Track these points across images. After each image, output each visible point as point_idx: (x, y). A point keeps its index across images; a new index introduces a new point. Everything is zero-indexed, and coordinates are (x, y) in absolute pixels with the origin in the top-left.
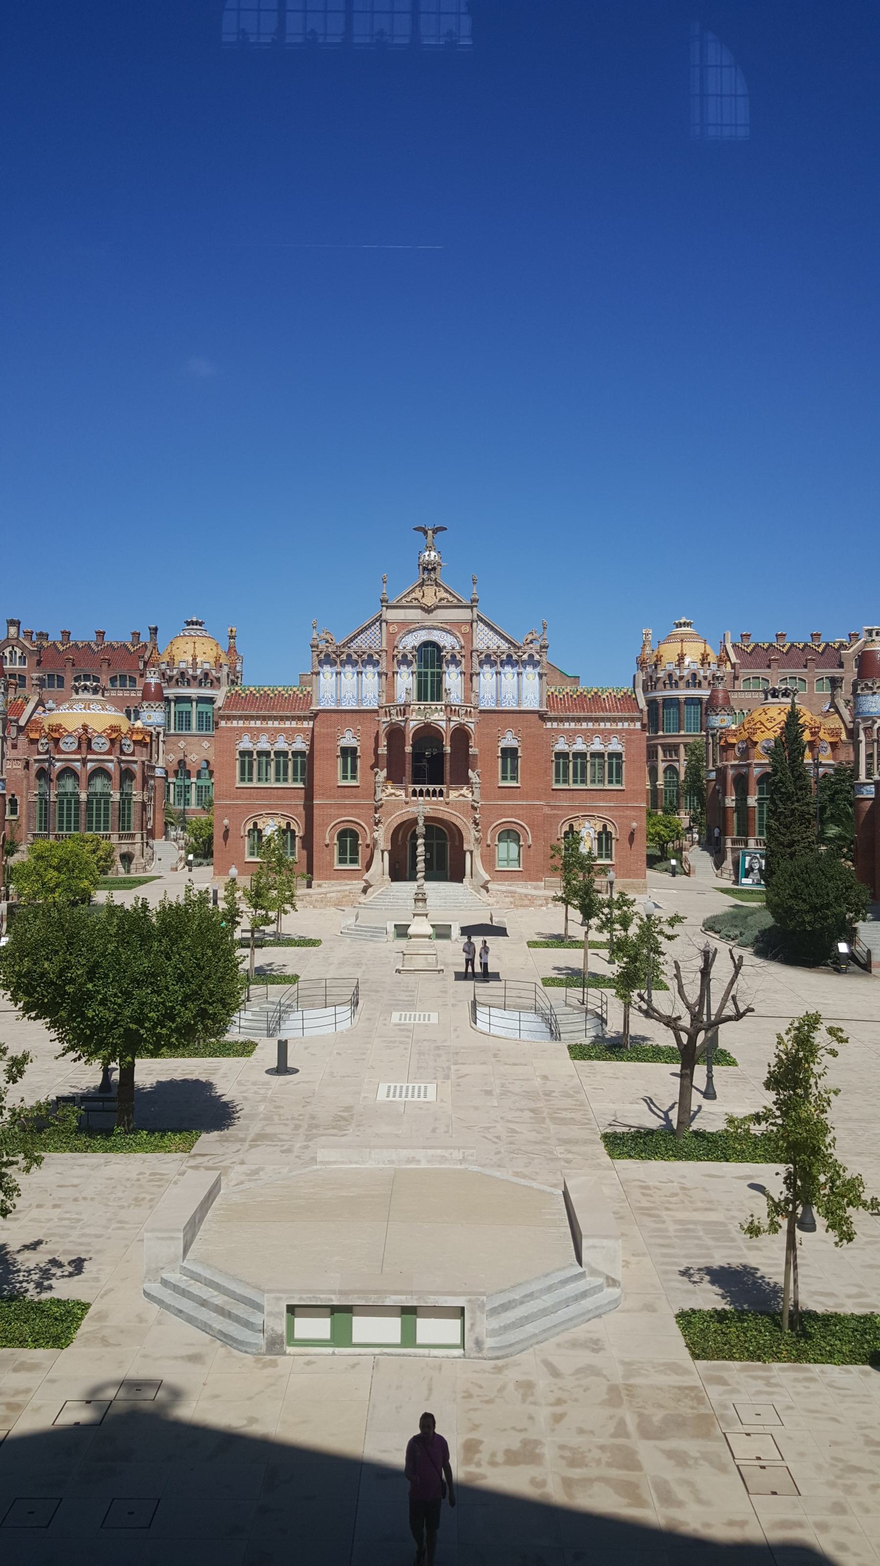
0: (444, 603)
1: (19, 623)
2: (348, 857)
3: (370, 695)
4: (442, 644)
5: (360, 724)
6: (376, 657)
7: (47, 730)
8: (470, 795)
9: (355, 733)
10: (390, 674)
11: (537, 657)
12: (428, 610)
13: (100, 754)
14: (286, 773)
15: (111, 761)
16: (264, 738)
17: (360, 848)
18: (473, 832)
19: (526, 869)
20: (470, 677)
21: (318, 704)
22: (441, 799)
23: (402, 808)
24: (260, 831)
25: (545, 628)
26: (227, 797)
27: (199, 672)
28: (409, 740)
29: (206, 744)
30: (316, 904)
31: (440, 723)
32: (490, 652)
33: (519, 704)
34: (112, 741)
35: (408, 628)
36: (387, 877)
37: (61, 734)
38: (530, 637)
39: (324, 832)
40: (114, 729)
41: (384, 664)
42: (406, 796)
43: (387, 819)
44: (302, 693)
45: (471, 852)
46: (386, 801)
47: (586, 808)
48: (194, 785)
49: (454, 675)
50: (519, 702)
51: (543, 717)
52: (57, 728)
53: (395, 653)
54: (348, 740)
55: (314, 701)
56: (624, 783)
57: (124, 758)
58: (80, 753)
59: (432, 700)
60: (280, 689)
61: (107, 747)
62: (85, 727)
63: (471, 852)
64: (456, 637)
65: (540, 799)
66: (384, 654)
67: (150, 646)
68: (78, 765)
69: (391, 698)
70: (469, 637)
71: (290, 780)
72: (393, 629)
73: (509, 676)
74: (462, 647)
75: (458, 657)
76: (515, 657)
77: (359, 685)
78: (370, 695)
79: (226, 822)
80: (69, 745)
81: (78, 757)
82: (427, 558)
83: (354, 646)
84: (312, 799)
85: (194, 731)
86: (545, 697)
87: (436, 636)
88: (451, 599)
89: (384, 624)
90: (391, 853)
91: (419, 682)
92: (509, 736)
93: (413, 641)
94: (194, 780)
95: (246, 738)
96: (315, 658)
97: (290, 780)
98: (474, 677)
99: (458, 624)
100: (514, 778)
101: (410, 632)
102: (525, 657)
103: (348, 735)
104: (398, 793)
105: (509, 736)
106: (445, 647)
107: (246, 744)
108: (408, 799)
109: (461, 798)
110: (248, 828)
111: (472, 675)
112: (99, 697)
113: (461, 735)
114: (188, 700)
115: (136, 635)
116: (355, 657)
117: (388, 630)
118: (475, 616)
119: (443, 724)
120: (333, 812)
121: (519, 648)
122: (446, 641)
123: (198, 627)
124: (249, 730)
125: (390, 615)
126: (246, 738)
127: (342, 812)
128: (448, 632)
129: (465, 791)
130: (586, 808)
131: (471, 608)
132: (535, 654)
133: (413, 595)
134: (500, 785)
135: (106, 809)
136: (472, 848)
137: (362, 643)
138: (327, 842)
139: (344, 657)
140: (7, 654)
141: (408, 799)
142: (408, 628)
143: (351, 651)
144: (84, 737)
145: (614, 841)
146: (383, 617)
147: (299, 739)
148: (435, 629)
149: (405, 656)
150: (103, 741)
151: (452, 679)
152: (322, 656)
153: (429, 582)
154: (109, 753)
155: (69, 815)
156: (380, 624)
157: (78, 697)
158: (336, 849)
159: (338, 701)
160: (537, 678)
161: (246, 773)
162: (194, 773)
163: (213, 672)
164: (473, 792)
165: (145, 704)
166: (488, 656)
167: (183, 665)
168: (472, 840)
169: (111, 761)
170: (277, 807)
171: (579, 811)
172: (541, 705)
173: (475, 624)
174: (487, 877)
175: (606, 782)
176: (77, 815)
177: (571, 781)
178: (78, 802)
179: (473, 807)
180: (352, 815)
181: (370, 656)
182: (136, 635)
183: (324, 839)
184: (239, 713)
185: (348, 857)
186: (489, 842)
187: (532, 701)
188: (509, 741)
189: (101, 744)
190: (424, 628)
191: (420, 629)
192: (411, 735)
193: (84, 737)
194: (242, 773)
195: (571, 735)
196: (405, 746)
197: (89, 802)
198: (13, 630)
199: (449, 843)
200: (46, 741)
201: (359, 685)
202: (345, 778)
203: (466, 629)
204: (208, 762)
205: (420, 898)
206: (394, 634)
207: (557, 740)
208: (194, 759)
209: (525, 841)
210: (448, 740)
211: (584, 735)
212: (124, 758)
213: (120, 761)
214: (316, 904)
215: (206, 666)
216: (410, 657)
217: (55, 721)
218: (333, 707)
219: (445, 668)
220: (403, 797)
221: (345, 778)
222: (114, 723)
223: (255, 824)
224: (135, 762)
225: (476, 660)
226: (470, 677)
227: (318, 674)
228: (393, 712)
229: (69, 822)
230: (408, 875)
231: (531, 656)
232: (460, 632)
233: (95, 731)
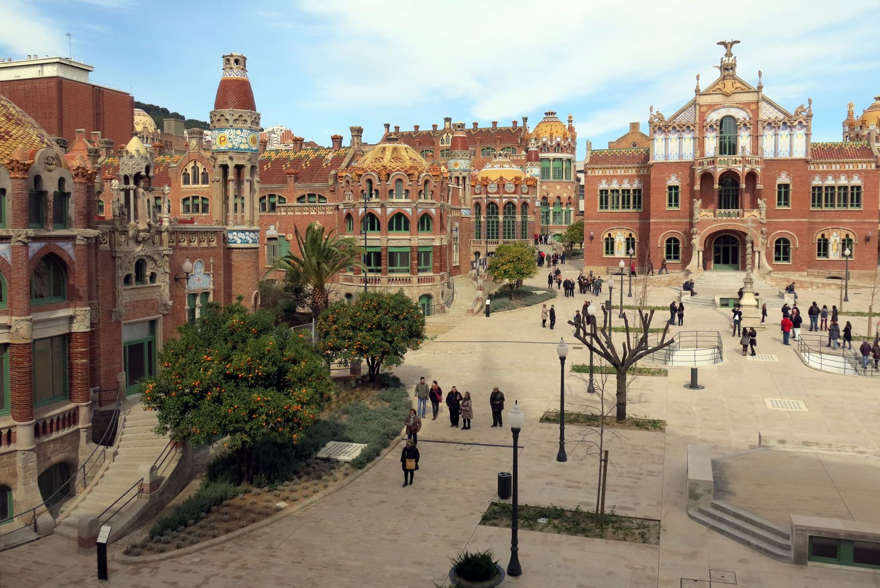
0: (739, 90)
1: (451, 119)
2: (672, 255)
3: (688, 153)
4: (737, 117)
5: (681, 171)
6: (692, 128)
7: (480, 180)
8: (758, 216)
9: (678, 177)
10: (701, 138)
11: (804, 123)
12: (727, 95)
13: (510, 193)
14: (628, 203)
15: (516, 198)
16: (615, 181)
17: (681, 250)
18: (760, 239)
19: (794, 263)
20: (756, 138)
21: (653, 159)
22: (739, 218)
23: (712, 224)
24: (612, 239)
25: (810, 104)
26: (593, 218)
27: (554, 143)
28: (717, 181)
29: (558, 187)
30: (656, 284)
31: (738, 169)
32: (771, 121)
33: (791, 155)
34: (516, 185)
35: (712, 107)
36: (701, 268)
37: (487, 182)
38: (800, 110)
39: (657, 240)
40: (517, 179)
41: (697, 132)
42: (715, 216)
43: (701, 231)
44: (637, 152)
45: (759, 252)
46: (701, 220)
47: (834, 223)
48: (551, 212)
49: (745, 138)
50: (791, 153)
51: (807, 162)
52: (486, 179)
53: (705, 125)
54: (673, 181)
55: (651, 157)
56: (862, 206)
57: (523, 196)
58: (499, 193)
59: (730, 154)
60: (623, 151)
61: (513, 190)
62: (501, 178)
63: (759, 252)
64: (747, 112)
65: (804, 218)
66: (697, 126)
67: (523, 130)
68: (497, 200)
69: (702, 154)
70: (756, 112)
71: (631, 208)
72: (703, 109)
73: (784, 137)
74: (750, 119)
75: (748, 125)
76: (788, 124)
77: (680, 146)
78: (688, 153)
79: (592, 233)
80: (492, 188)
81: (498, 196)
82: (727, 62)
83: (677, 121)
84: (649, 219)
85: (552, 180)
86: (810, 151)
87: (733, 112)
88: (743, 88)
89: (697, 107)
90: (703, 252)
91: (721, 143)
92: (784, 175)
93: (715, 116)
94: (551, 208)
95: (604, 182)
96: (652, 130)
97: (631, 208)
98: (760, 138)
99: (748, 104)
100: (786, 204)
101: (714, 110)
102: (796, 123)
103: (673, 178)
104: (709, 214)
105: (784, 175)
106: (738, 119)
107: (603, 185)
108: (716, 219)
109: (753, 218)
110: (605, 237)
111: (757, 137)
112: (508, 160)
113: (752, 176)
114: (548, 159)
115: (515, 123)
116: (678, 128)
117: (700, 109)
118: (760, 98)
119: (740, 169)
120: (663, 227)
121: (791, 117)
122: (741, 115)
123: (553, 116)
124: (605, 177)
125: (703, 100)
126: (604, 182)
127: (669, 227)
128: (742, 109)
129: (755, 212)
130: (834, 223)
131: (758, 92)
132: (802, 121)
133: (717, 87)
134: (777, 208)
135: (513, 226)
136: (760, 250)
137: (683, 119)
138: (659, 246)
139: (670, 128)
140: (445, 138)
141: (716, 219)
142: (712, 107)
143: (675, 125)
144: (501, 184)
145: (854, 245)
146: (697, 102)
147: (637, 181)
148: (732, 107)
149: (711, 126)
150: (511, 185)
151: (744, 140)
152: (656, 128)
153: (729, 77)
154: (515, 193)
155: (493, 230)
156: (695, 106)
157: (496, 161)
158: (665, 250)
159: (666, 157)
160: (804, 136)
161: (604, 202)
162: (551, 204)
163: (563, 143)
164: (761, 214)
165: (529, 163)
166: (770, 124)
167: (545, 139)
168: (760, 244)
169: (516, 198)
170: (623, 224)
171: (829, 225)
172: (807, 155)
173: (760, 103)
174: (770, 269)
175: (849, 206)
176: (505, 230)
177: (823, 205)
178: (497, 222)
179: (760, 222)
180: (675, 229)
181: (688, 127)
182: (515, 123)
183: (657, 244)
184: (599, 166)
185: (672, 255)
186: (769, 246)
187: (800, 152)
188: (783, 179)
189: (510, 187)
190: (725, 107)
191: (722, 108)
192: (718, 177)
193: (501, 184)
194: (601, 203)
195: (824, 175)
196: (713, 184)
197: (504, 222)
198: (447, 124)
199: (740, 247)
200: (479, 186)
201: (680, 146)
202: (670, 205)
203: (753, 107)
204: (559, 198)
205: (748, 281)
206: (705, 113)
207: (814, 178)
208: (552, 196)
209: (794, 245)
210: (744, 180)
211: (834, 174)
212: (523, 196)
213: (521, 198)
214: (656, 284)
215: (558, 139)
216: (715, 127)
217: (485, 176)
218: (662, 160)
219: (739, 131)
220: (712, 217)
221: (670, 205)
222: (517, 175)
223: (610, 235)
224: (529, 198)
225: (760, 126)
226: (756, 138)
227: (654, 139)
228: (706, 163)
229: (493, 234)
230: (712, 266)
231: (800, 123)
232: (750, 109)
233: (507, 180)
